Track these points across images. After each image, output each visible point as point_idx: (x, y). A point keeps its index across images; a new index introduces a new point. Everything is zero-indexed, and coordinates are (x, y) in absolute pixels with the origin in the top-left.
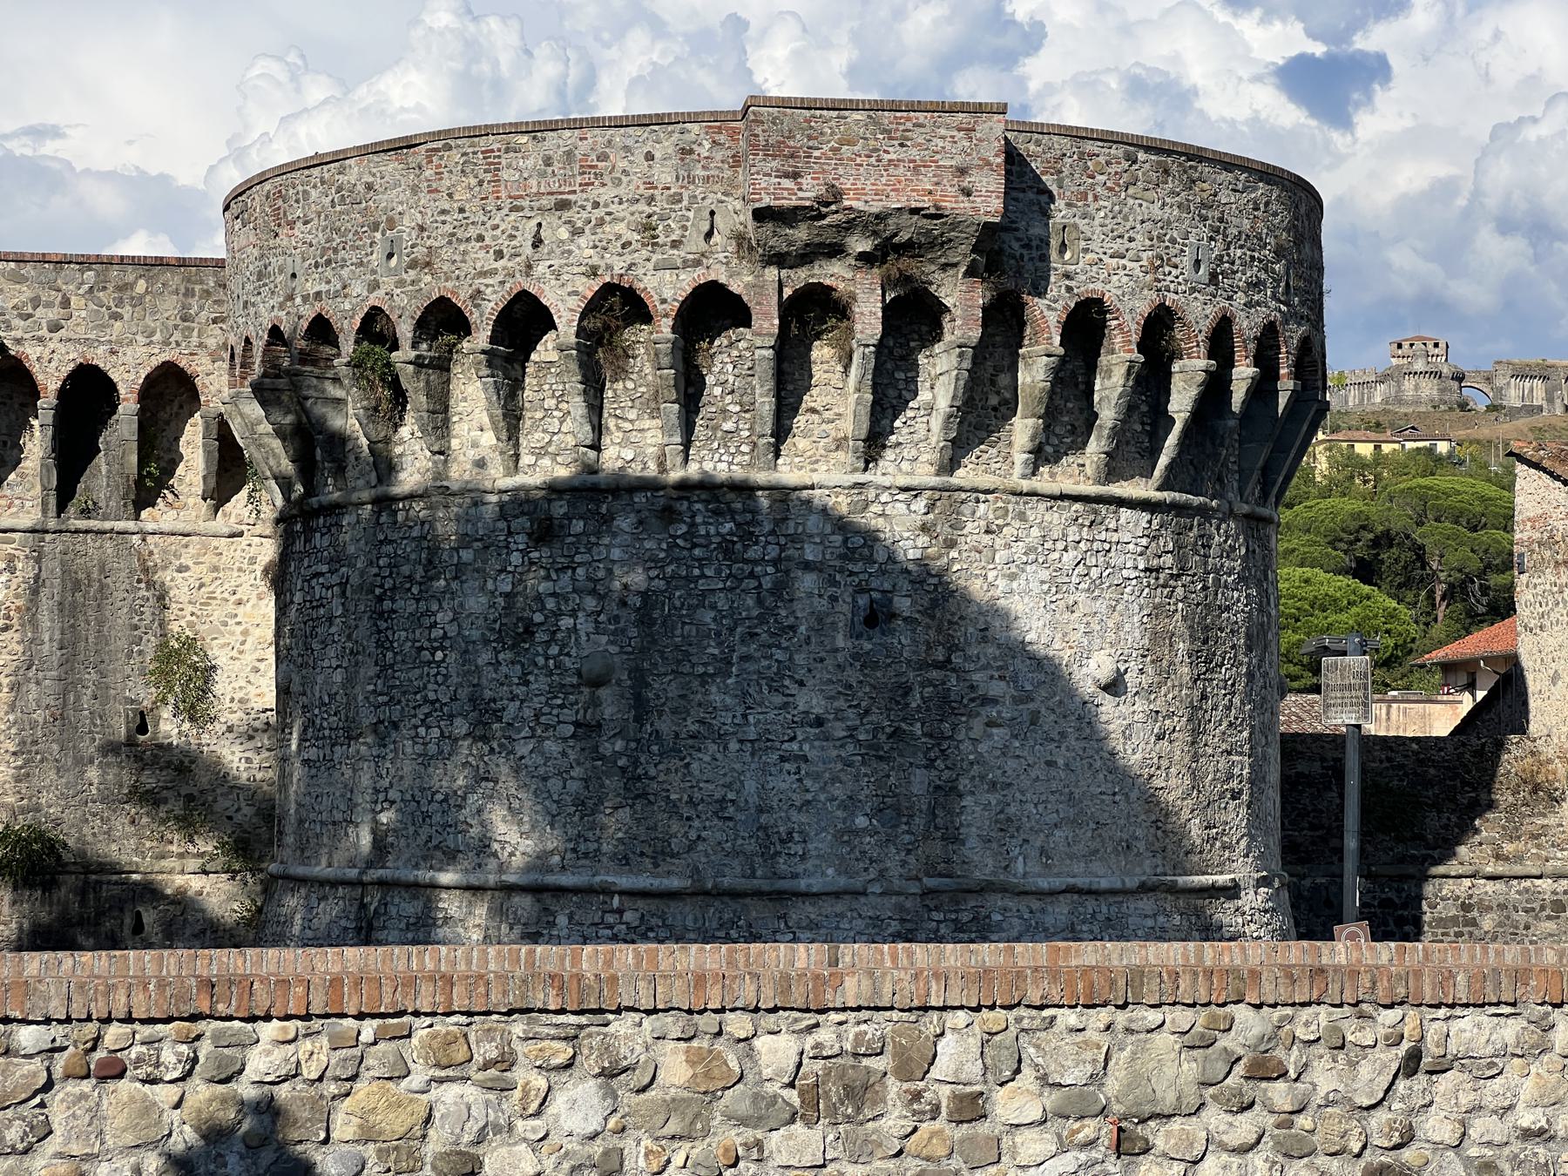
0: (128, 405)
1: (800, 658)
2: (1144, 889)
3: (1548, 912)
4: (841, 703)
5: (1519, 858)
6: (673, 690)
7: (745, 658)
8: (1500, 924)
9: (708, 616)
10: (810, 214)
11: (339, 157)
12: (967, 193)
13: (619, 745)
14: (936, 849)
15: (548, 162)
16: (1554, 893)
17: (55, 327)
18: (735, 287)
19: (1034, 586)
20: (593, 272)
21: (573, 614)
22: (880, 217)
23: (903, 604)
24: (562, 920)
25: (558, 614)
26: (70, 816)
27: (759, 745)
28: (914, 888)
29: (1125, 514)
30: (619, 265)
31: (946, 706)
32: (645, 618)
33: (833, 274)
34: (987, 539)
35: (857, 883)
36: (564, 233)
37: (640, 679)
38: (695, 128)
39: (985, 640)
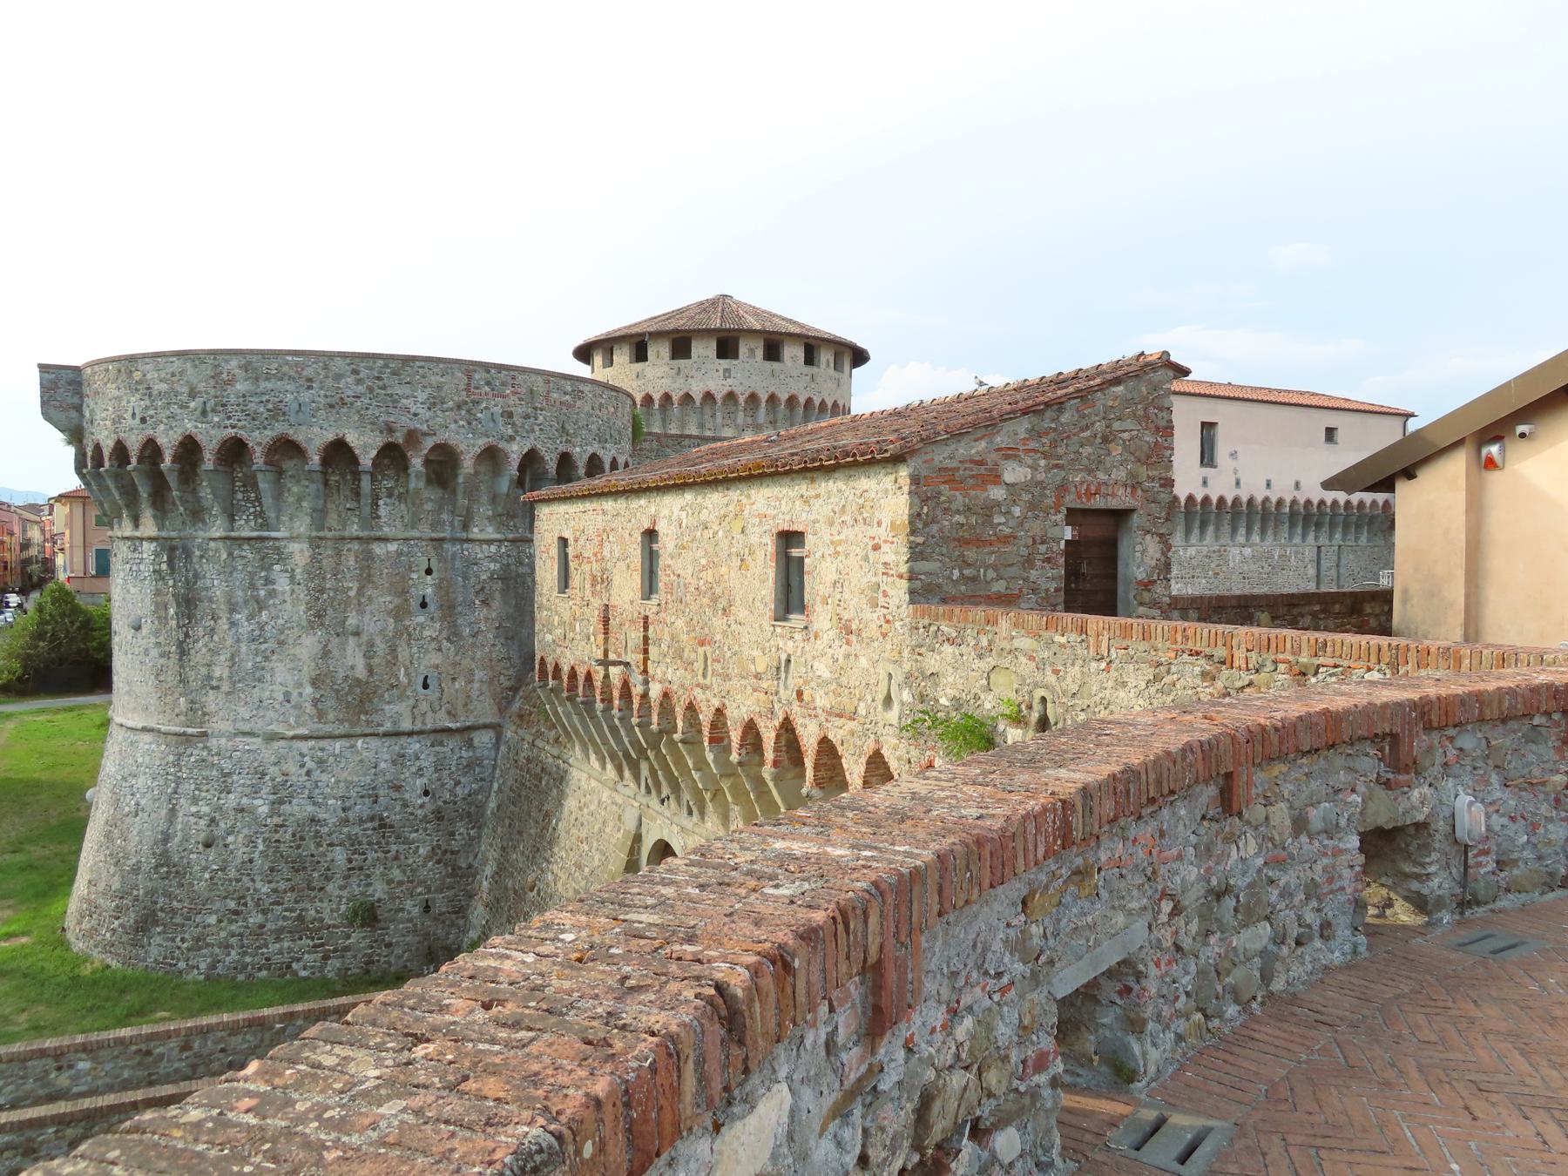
2: (144, 729)
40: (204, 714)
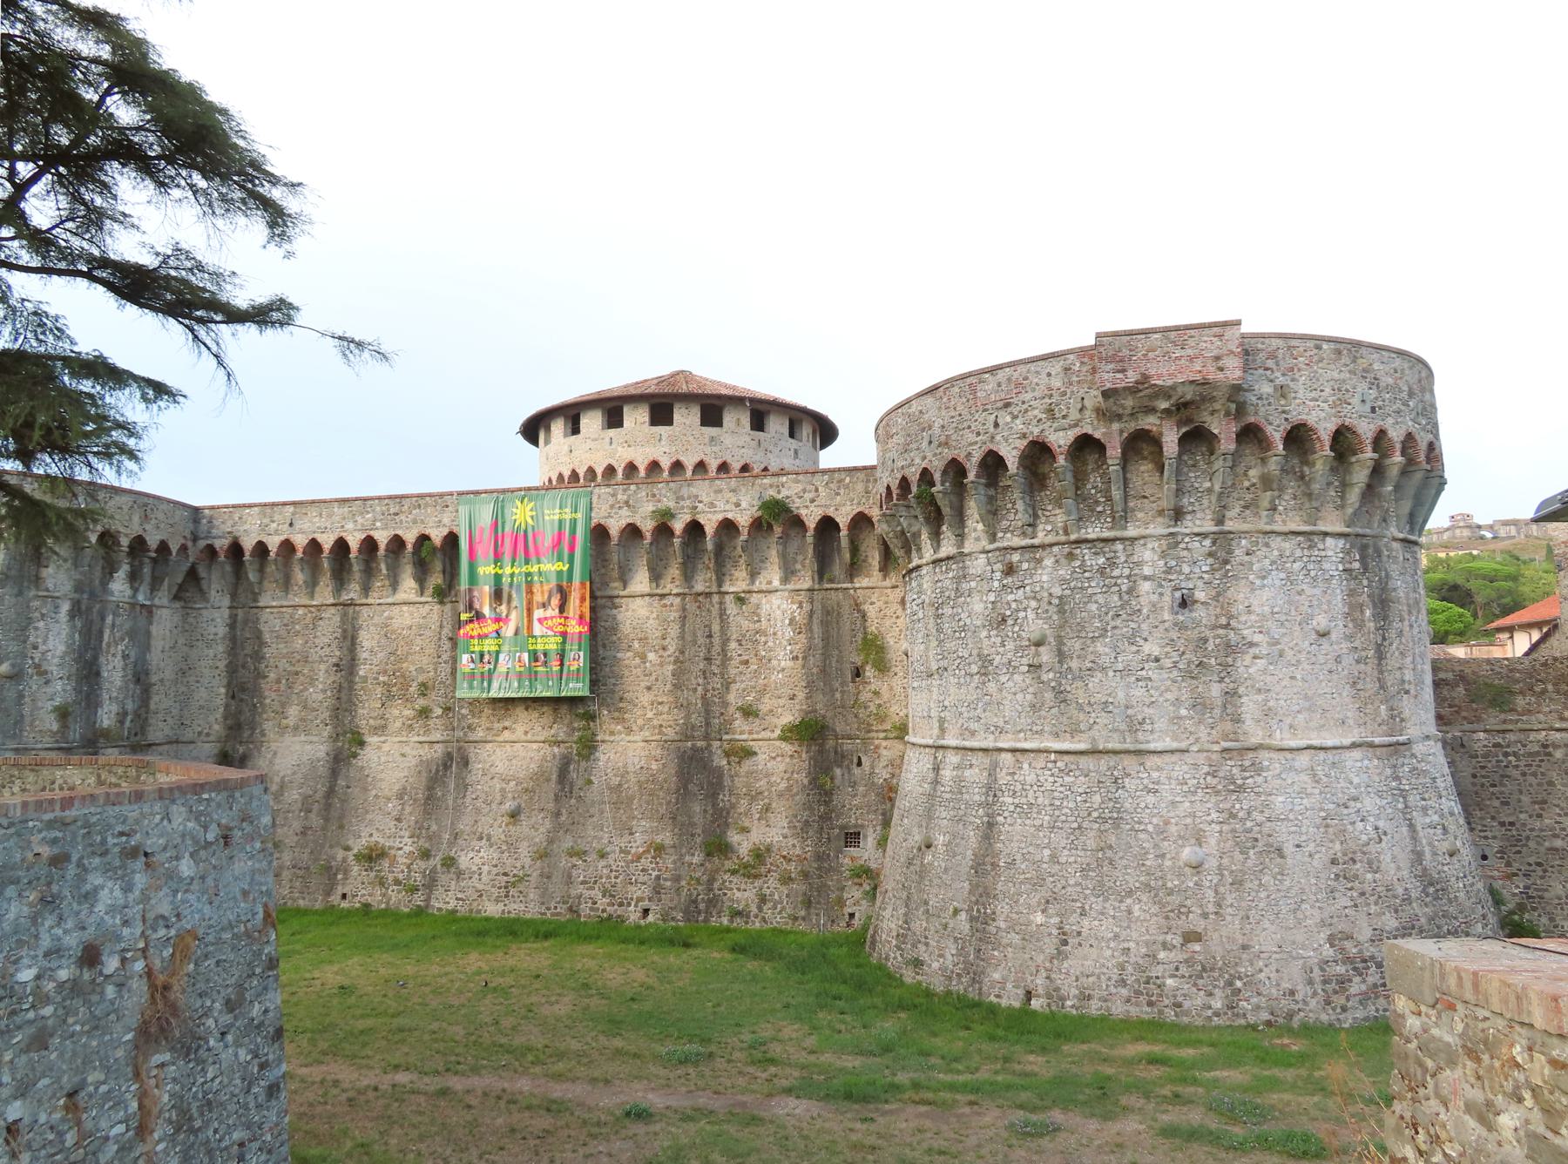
0: (844, 533)
1: (1144, 626)
2: (1354, 746)
4: (1168, 649)
6: (1077, 646)
7: (1115, 628)
9: (1094, 607)
10: (1133, 390)
11: (908, 401)
12: (1221, 369)
13: (1051, 675)
14: (1228, 726)
15: (999, 385)
17: (813, 501)
18: (1097, 435)
19: (1278, 583)
20: (1024, 436)
21: (1025, 610)
22: (1174, 387)
23: (1200, 595)
24: (1026, 766)
25: (1018, 610)
26: (829, 714)
27: (1125, 672)
28: (1216, 748)
29: (1329, 540)
30: (1036, 431)
31: (1229, 649)
32: (1061, 611)
33: (1150, 422)
34: (1247, 558)
35: (1183, 745)
36: (1008, 419)
37: (1060, 641)
38: (1071, 357)
39: (1249, 612)
40: (1402, 720)
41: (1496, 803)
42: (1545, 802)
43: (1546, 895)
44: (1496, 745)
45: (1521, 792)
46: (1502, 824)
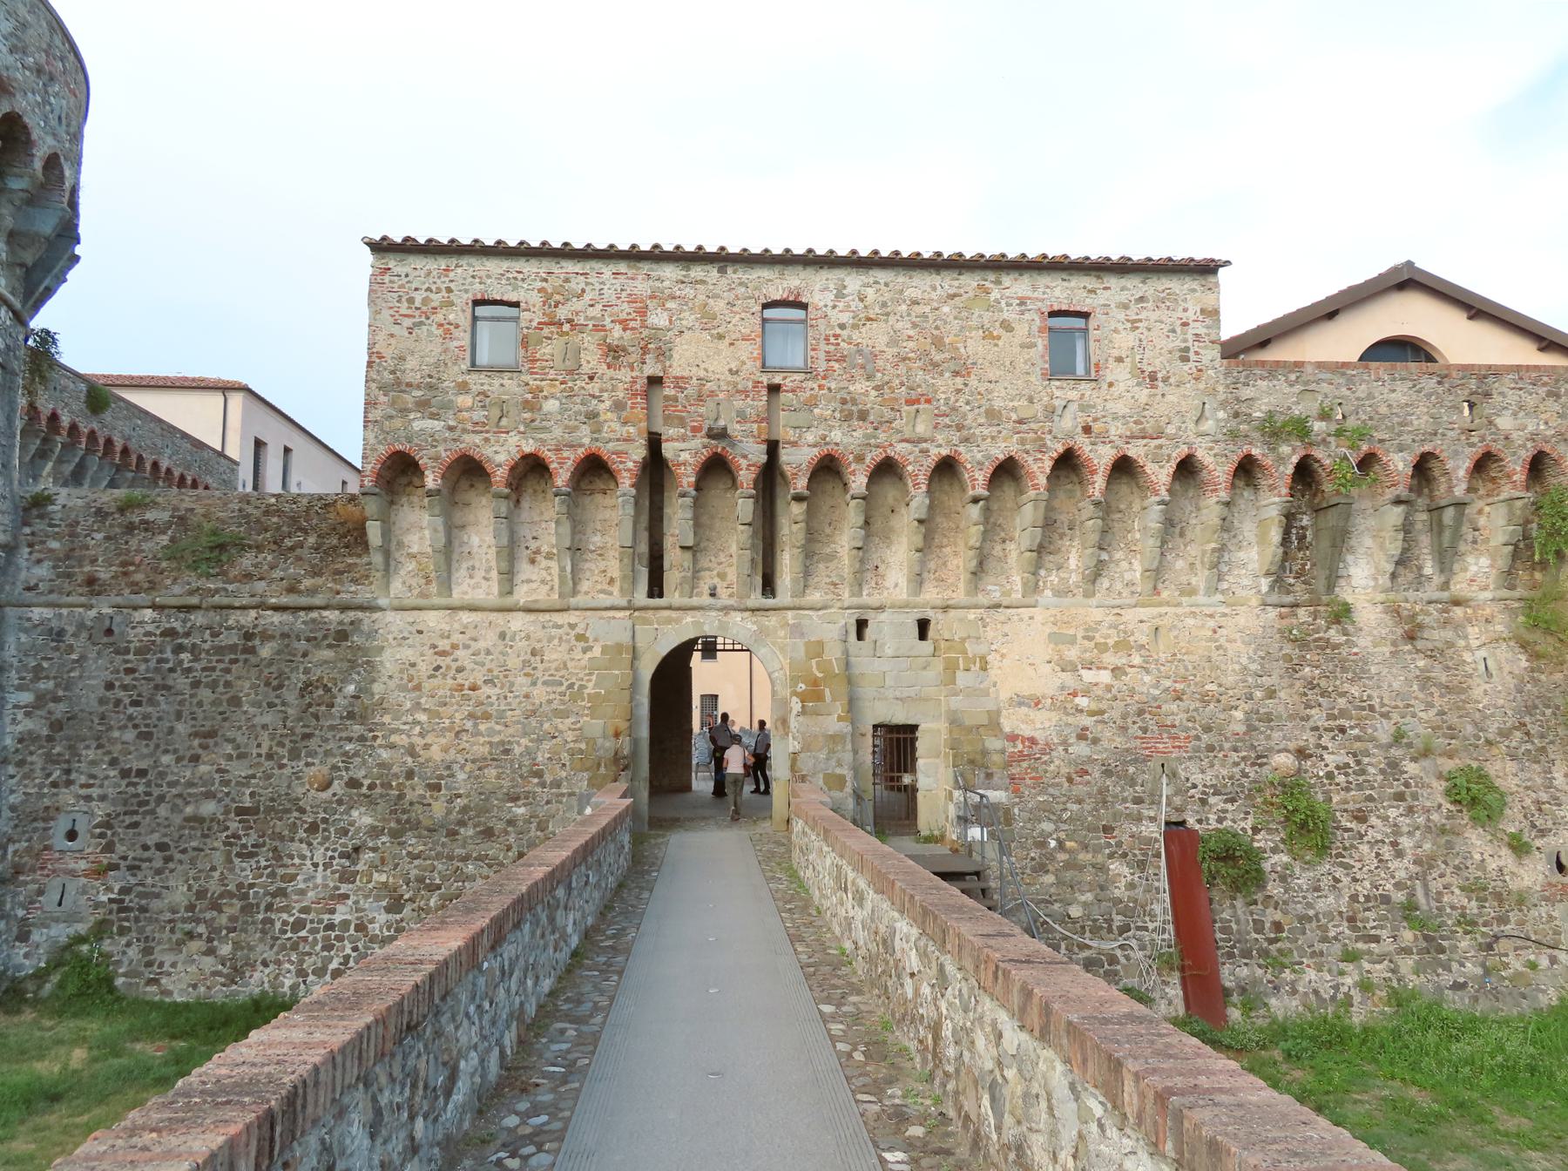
3: (330, 640)
5: (312, 591)
8: (279, 652)
16: (341, 623)
41: (130, 735)
42: (212, 734)
43: (155, 904)
44: (170, 633)
45: (179, 716)
46: (125, 774)
